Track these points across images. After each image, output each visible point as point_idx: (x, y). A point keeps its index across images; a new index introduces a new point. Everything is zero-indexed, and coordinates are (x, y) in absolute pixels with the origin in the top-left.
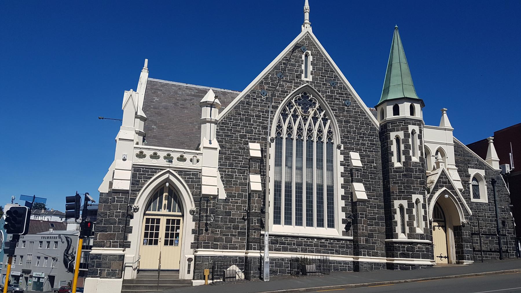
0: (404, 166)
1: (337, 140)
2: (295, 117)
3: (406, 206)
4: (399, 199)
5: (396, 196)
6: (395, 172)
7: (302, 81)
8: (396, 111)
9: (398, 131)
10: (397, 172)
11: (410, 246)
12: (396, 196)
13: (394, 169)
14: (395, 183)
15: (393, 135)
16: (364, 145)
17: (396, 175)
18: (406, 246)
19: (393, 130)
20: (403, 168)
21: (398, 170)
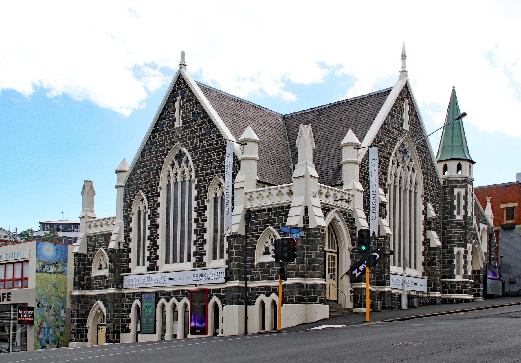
0: (463, 219)
1: (421, 190)
2: (398, 165)
3: (463, 253)
4: (458, 247)
5: (456, 244)
6: (456, 223)
7: (403, 129)
8: (459, 167)
9: (460, 188)
10: (458, 224)
11: (464, 284)
12: (456, 244)
13: (455, 220)
14: (455, 233)
15: (456, 191)
16: (433, 196)
17: (457, 226)
18: (461, 285)
19: (456, 187)
20: (463, 221)
21: (459, 222)
